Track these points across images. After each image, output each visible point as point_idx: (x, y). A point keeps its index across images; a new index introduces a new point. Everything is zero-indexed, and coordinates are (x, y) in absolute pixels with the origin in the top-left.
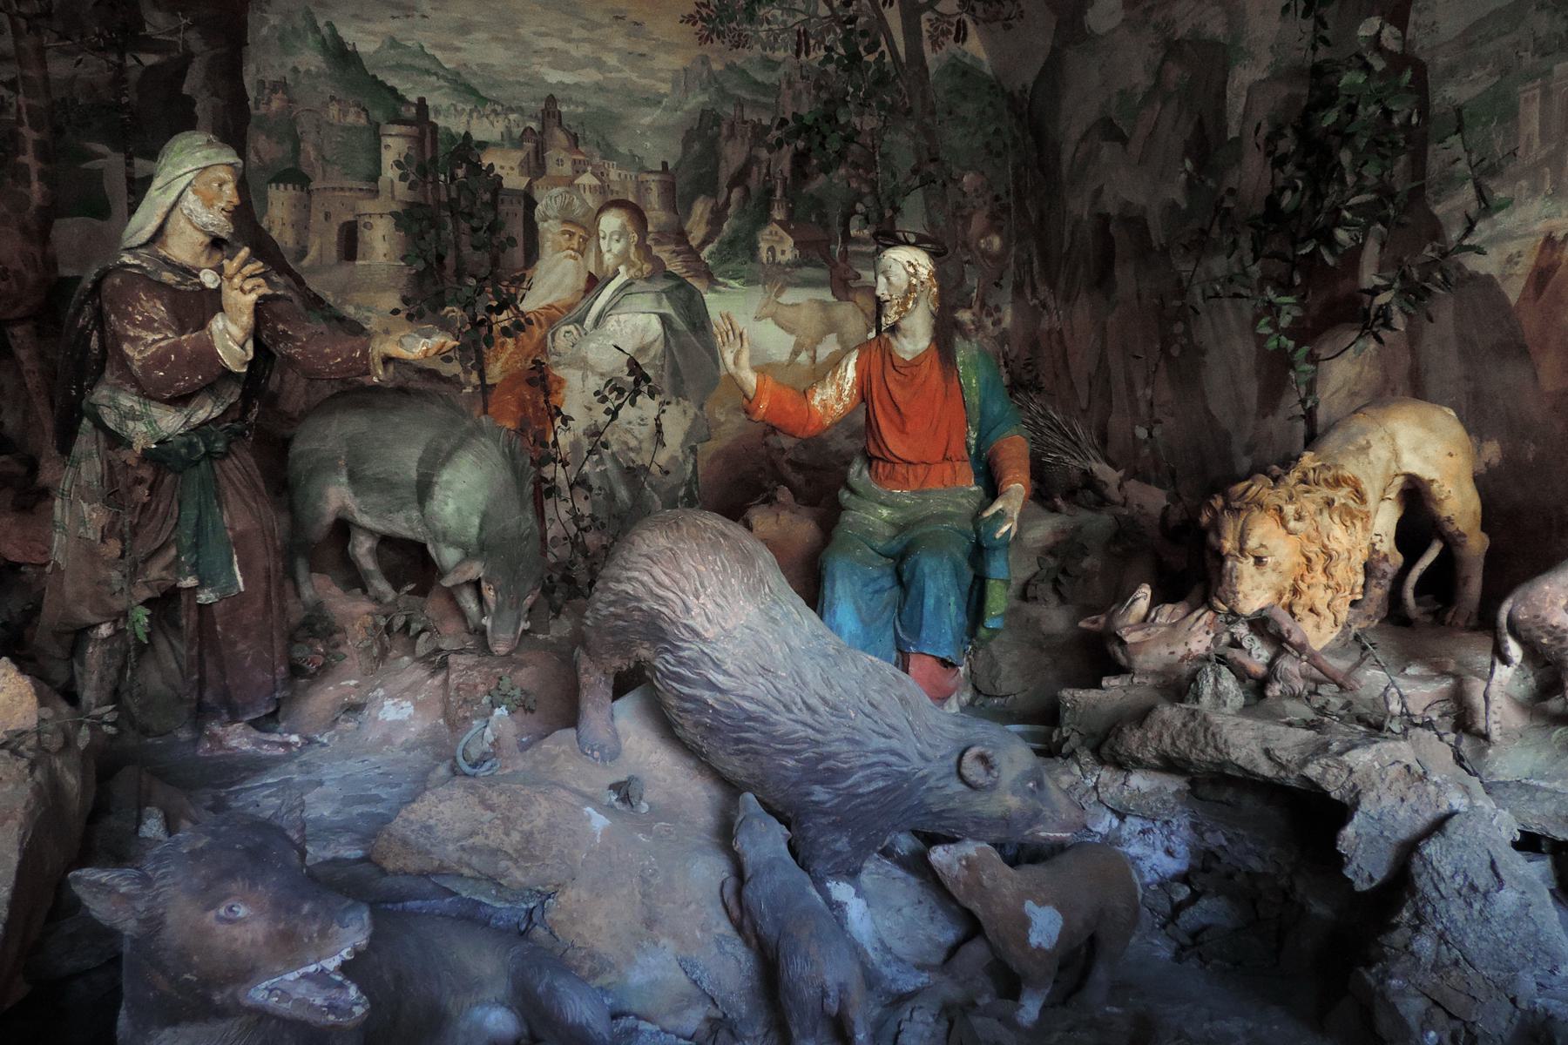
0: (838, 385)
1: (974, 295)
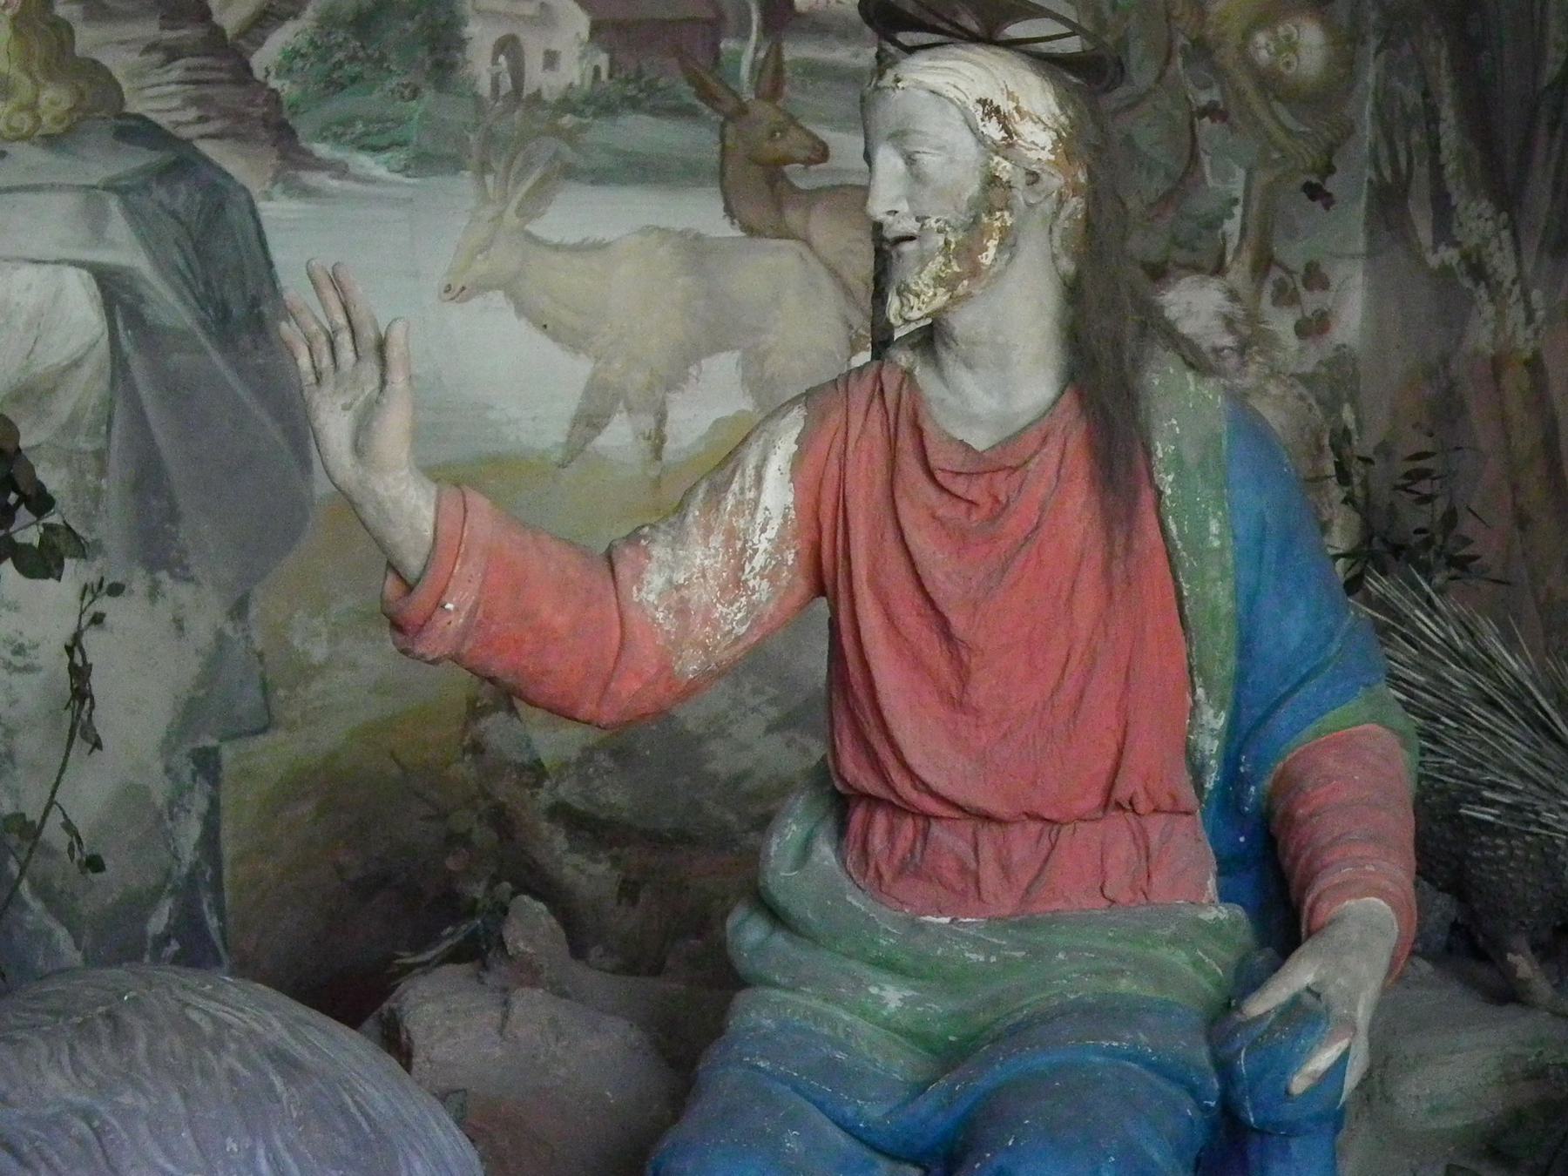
0: (731, 534)
1: (1232, 226)
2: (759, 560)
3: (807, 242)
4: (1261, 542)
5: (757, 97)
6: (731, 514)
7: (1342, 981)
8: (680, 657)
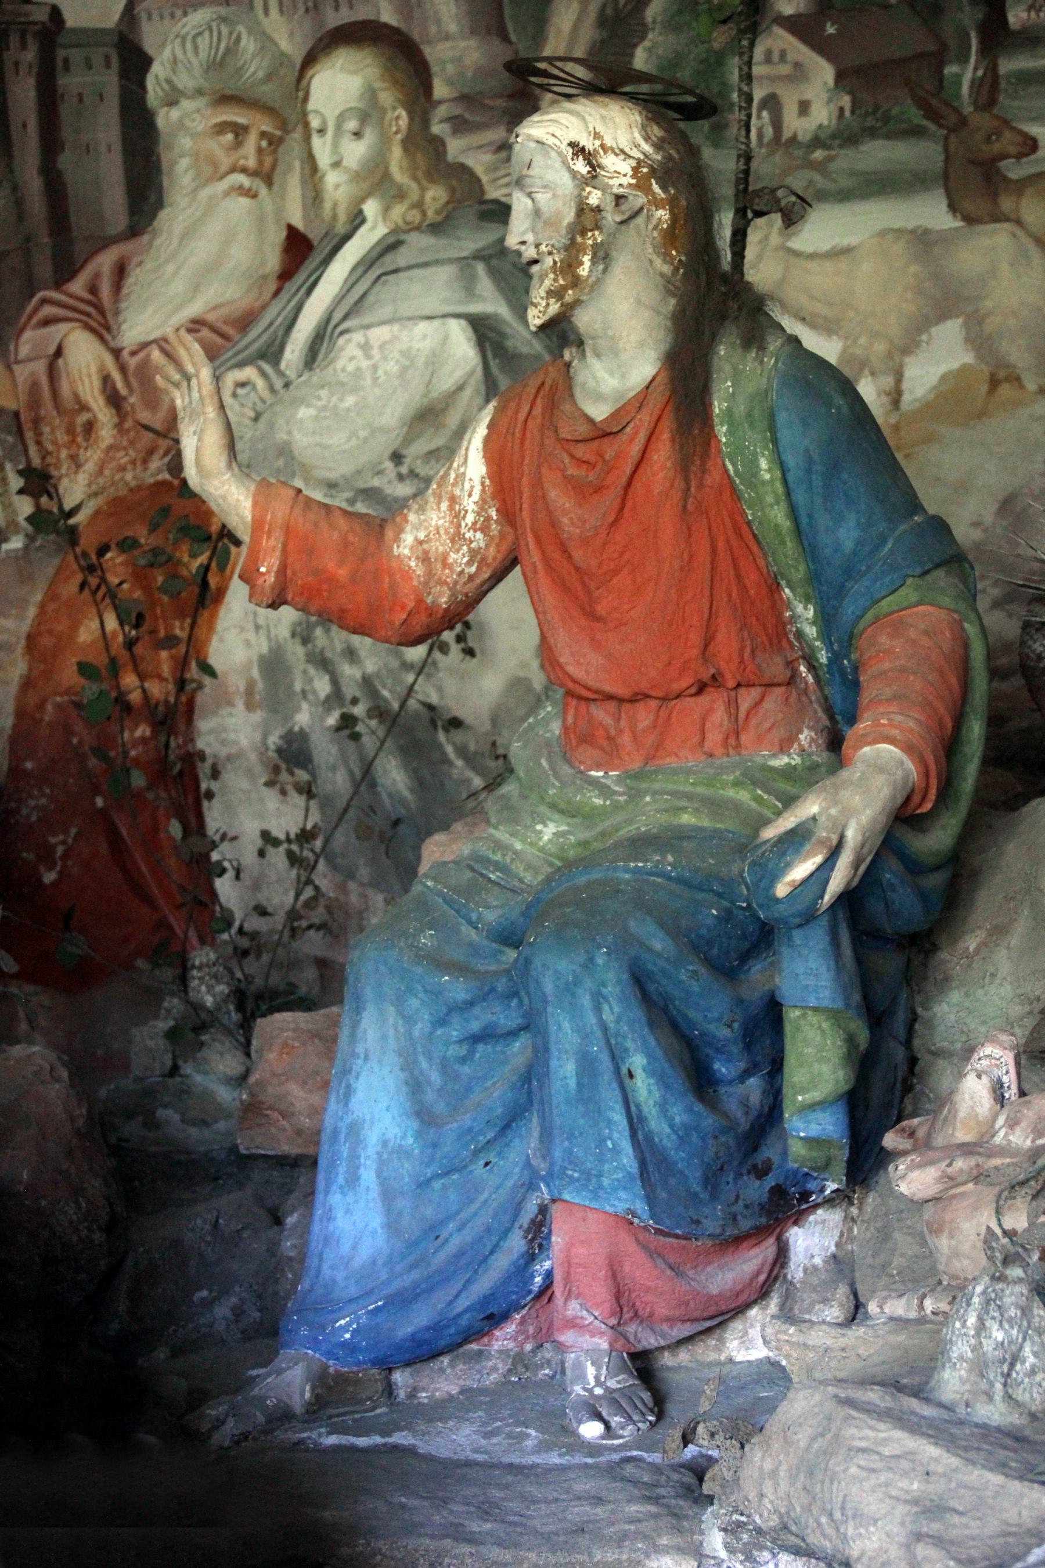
2: (470, 518)
3: (1019, 223)
4: (809, 471)
5: (976, 109)
6: (454, 485)
7: (833, 811)
8: (429, 594)
